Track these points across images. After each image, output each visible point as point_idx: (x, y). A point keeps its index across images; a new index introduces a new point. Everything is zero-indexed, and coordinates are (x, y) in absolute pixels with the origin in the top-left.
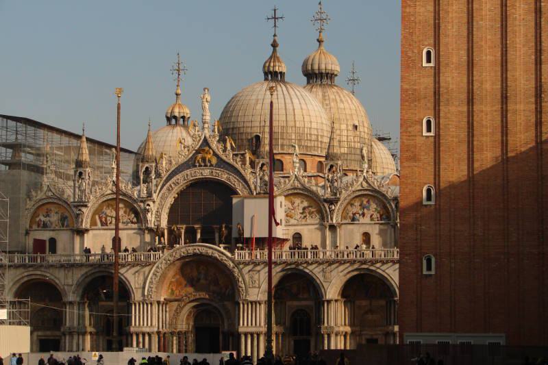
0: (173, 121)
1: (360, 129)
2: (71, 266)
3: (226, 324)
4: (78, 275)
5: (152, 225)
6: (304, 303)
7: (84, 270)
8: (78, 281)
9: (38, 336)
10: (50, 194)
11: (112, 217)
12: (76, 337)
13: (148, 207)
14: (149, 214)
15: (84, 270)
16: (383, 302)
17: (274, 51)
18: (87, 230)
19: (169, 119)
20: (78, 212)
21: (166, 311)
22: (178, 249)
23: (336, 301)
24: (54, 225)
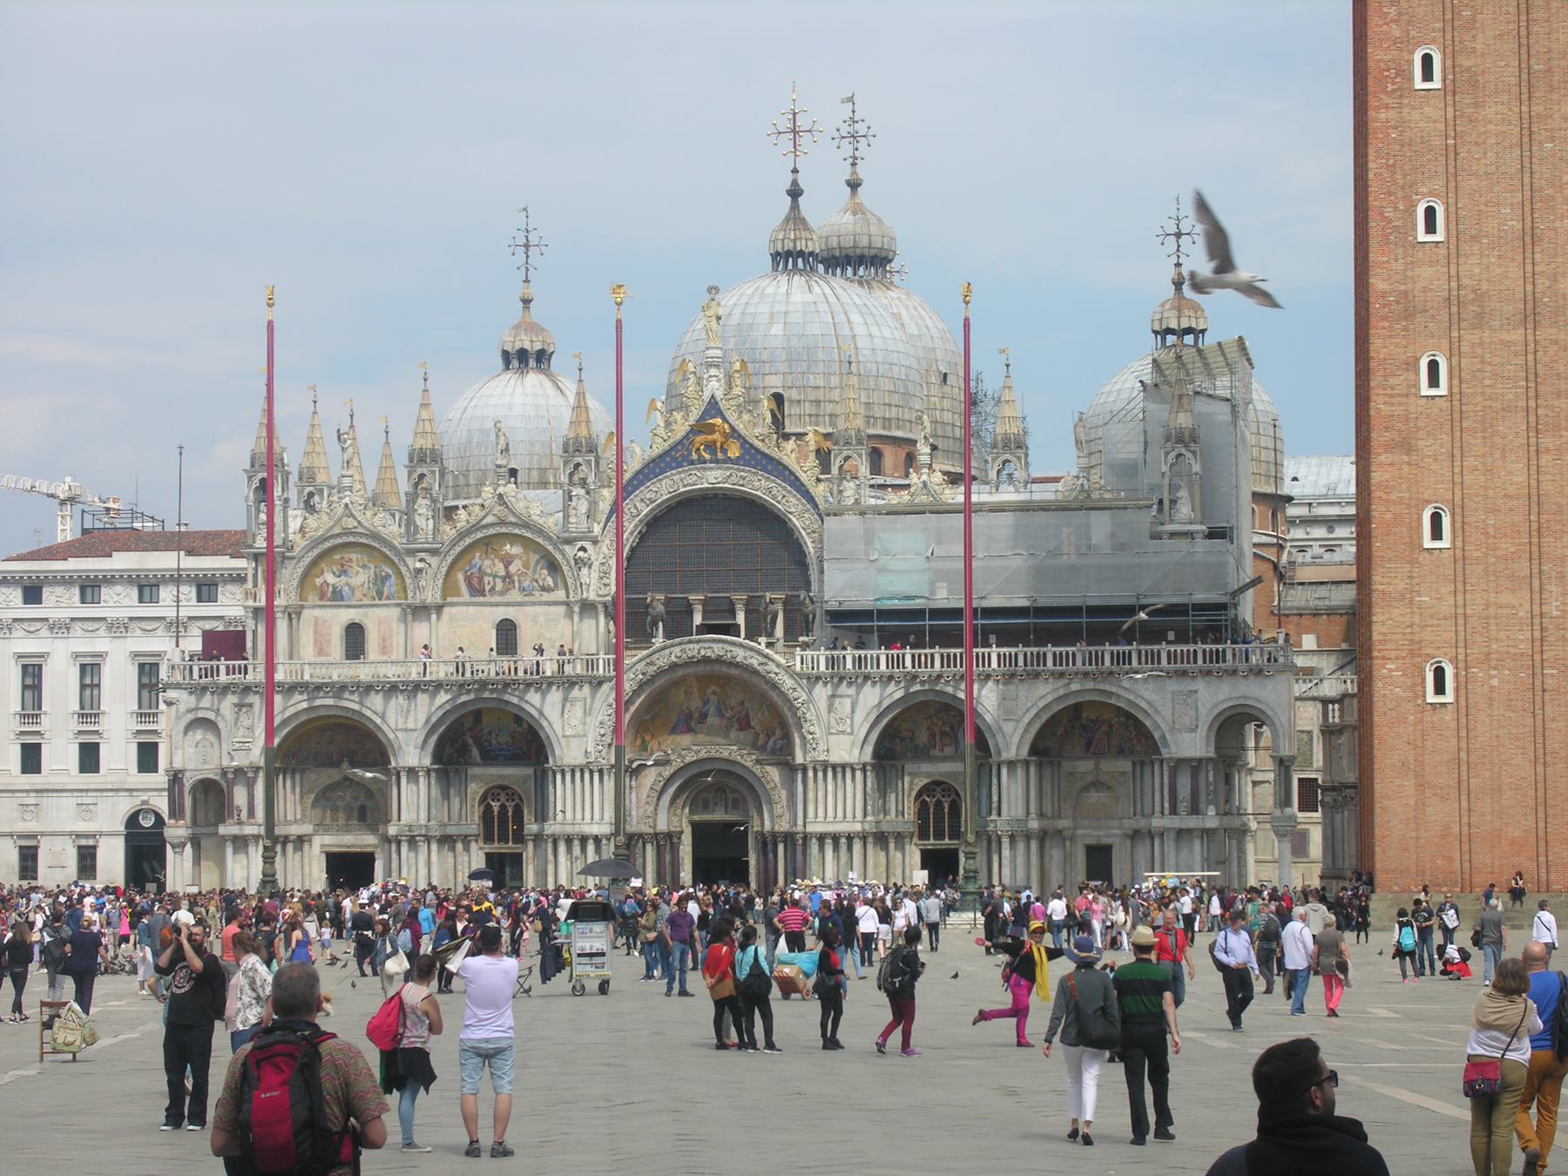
0: (515, 363)
1: (951, 379)
6: (945, 767)
7: (443, 697)
8: (428, 721)
9: (322, 846)
10: (351, 523)
11: (495, 577)
12: (423, 847)
13: (581, 554)
14: (585, 571)
15: (443, 697)
16: (1125, 765)
17: (795, 206)
18: (439, 608)
19: (506, 356)
20: (419, 565)
23: (1027, 763)
24: (358, 594)
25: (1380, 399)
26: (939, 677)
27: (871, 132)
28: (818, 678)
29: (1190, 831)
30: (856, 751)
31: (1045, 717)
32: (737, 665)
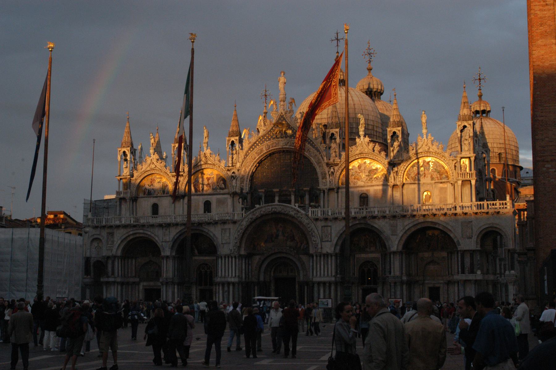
2: (168, 225)
3: (301, 275)
4: (173, 232)
5: (238, 191)
6: (371, 256)
7: (180, 228)
8: (174, 237)
9: (143, 286)
10: (153, 166)
13: (233, 175)
14: (234, 181)
15: (180, 228)
16: (445, 254)
21: (249, 264)
22: (258, 208)
23: (401, 253)
24: (156, 193)
25: (537, 8)
26: (365, 218)
27: (375, 52)
28: (317, 220)
29: (470, 281)
30: (333, 248)
31: (409, 233)
32: (287, 215)
